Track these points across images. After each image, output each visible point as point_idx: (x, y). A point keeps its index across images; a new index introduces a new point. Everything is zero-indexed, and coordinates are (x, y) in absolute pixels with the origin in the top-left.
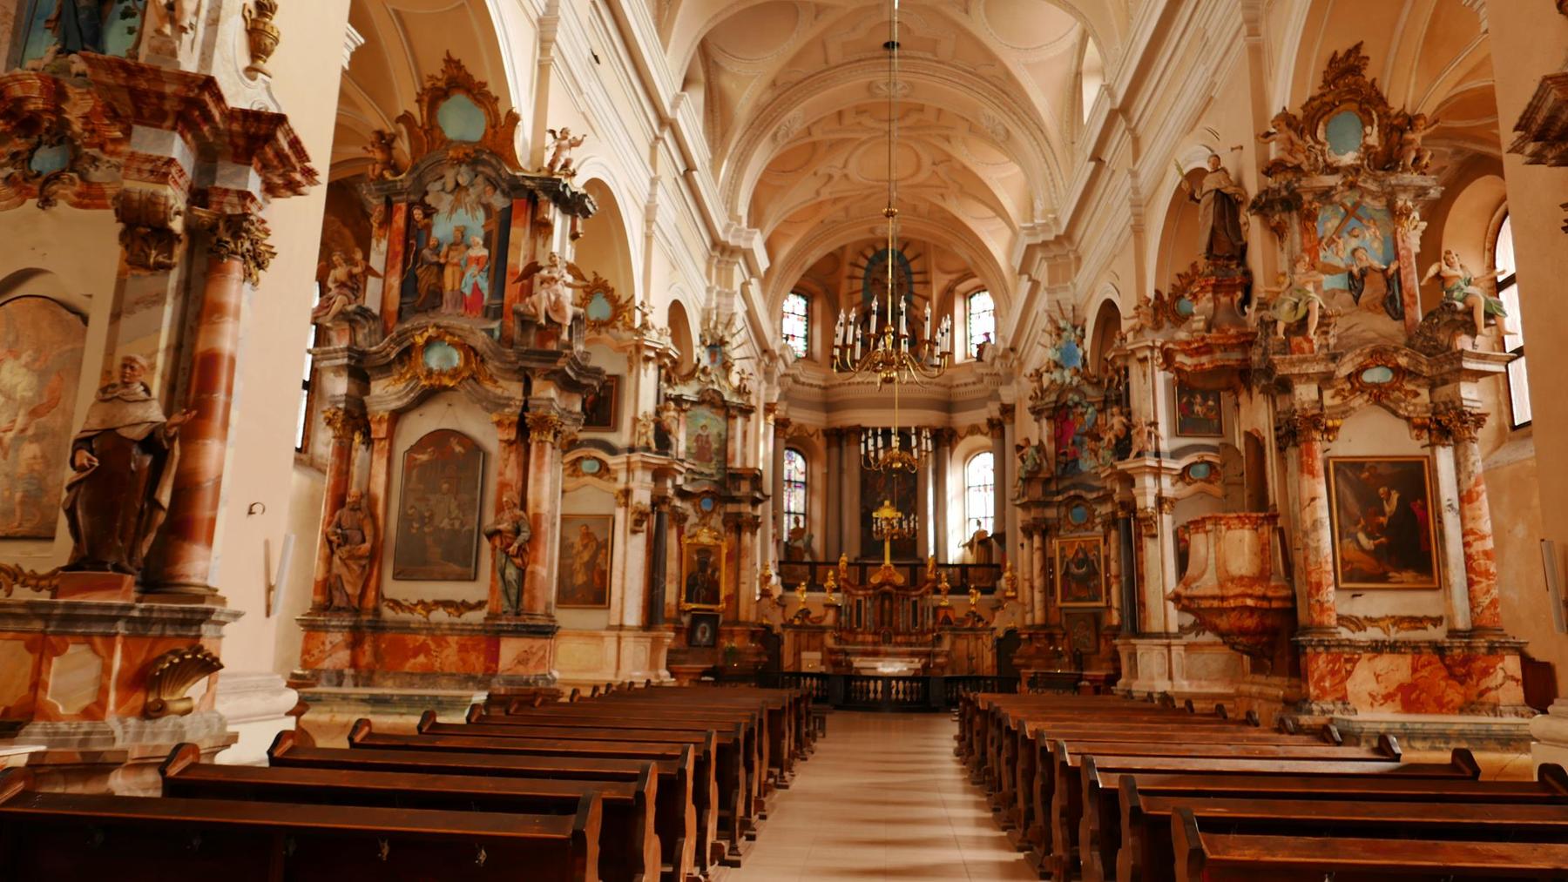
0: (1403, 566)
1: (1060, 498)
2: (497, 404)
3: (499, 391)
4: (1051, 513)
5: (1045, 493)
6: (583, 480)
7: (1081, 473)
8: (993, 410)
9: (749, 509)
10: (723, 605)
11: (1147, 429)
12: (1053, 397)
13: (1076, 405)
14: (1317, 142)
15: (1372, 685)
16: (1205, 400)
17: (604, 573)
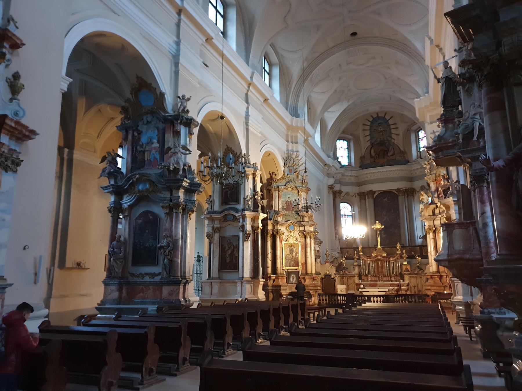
2: (163, 200)
3: (162, 196)
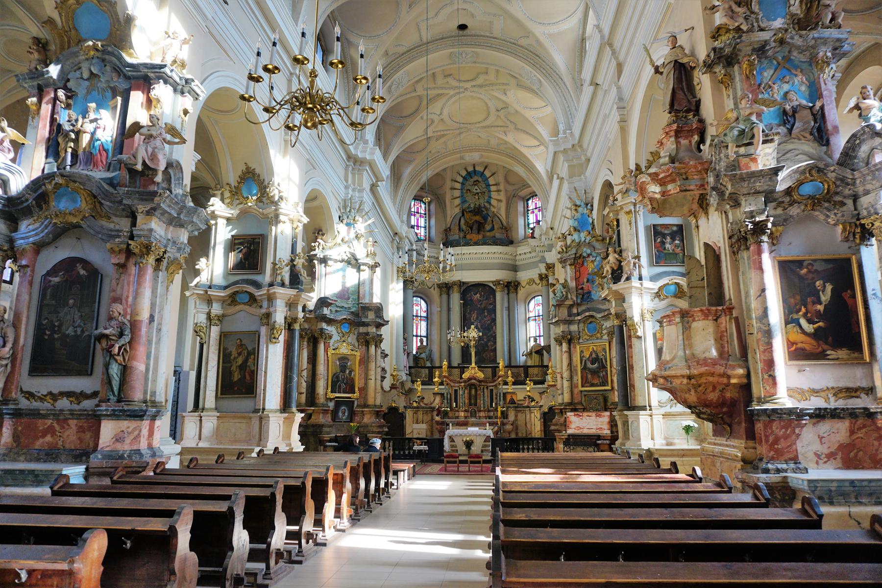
0: (836, 346)
1: (579, 318)
2: (112, 235)
3: (112, 226)
4: (574, 328)
5: (570, 315)
6: (238, 308)
7: (592, 300)
8: (542, 269)
9: (374, 330)
10: (357, 395)
11: (632, 261)
12: (574, 251)
13: (589, 255)
14: (752, 13)
15: (817, 447)
16: (673, 239)
17: (253, 372)
